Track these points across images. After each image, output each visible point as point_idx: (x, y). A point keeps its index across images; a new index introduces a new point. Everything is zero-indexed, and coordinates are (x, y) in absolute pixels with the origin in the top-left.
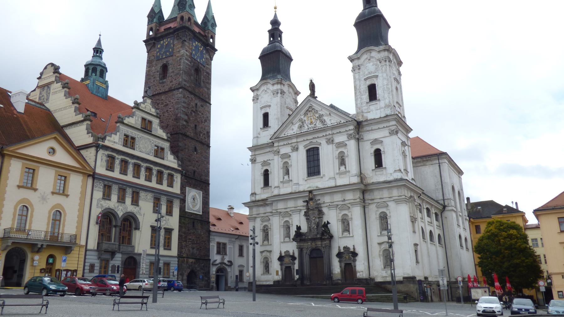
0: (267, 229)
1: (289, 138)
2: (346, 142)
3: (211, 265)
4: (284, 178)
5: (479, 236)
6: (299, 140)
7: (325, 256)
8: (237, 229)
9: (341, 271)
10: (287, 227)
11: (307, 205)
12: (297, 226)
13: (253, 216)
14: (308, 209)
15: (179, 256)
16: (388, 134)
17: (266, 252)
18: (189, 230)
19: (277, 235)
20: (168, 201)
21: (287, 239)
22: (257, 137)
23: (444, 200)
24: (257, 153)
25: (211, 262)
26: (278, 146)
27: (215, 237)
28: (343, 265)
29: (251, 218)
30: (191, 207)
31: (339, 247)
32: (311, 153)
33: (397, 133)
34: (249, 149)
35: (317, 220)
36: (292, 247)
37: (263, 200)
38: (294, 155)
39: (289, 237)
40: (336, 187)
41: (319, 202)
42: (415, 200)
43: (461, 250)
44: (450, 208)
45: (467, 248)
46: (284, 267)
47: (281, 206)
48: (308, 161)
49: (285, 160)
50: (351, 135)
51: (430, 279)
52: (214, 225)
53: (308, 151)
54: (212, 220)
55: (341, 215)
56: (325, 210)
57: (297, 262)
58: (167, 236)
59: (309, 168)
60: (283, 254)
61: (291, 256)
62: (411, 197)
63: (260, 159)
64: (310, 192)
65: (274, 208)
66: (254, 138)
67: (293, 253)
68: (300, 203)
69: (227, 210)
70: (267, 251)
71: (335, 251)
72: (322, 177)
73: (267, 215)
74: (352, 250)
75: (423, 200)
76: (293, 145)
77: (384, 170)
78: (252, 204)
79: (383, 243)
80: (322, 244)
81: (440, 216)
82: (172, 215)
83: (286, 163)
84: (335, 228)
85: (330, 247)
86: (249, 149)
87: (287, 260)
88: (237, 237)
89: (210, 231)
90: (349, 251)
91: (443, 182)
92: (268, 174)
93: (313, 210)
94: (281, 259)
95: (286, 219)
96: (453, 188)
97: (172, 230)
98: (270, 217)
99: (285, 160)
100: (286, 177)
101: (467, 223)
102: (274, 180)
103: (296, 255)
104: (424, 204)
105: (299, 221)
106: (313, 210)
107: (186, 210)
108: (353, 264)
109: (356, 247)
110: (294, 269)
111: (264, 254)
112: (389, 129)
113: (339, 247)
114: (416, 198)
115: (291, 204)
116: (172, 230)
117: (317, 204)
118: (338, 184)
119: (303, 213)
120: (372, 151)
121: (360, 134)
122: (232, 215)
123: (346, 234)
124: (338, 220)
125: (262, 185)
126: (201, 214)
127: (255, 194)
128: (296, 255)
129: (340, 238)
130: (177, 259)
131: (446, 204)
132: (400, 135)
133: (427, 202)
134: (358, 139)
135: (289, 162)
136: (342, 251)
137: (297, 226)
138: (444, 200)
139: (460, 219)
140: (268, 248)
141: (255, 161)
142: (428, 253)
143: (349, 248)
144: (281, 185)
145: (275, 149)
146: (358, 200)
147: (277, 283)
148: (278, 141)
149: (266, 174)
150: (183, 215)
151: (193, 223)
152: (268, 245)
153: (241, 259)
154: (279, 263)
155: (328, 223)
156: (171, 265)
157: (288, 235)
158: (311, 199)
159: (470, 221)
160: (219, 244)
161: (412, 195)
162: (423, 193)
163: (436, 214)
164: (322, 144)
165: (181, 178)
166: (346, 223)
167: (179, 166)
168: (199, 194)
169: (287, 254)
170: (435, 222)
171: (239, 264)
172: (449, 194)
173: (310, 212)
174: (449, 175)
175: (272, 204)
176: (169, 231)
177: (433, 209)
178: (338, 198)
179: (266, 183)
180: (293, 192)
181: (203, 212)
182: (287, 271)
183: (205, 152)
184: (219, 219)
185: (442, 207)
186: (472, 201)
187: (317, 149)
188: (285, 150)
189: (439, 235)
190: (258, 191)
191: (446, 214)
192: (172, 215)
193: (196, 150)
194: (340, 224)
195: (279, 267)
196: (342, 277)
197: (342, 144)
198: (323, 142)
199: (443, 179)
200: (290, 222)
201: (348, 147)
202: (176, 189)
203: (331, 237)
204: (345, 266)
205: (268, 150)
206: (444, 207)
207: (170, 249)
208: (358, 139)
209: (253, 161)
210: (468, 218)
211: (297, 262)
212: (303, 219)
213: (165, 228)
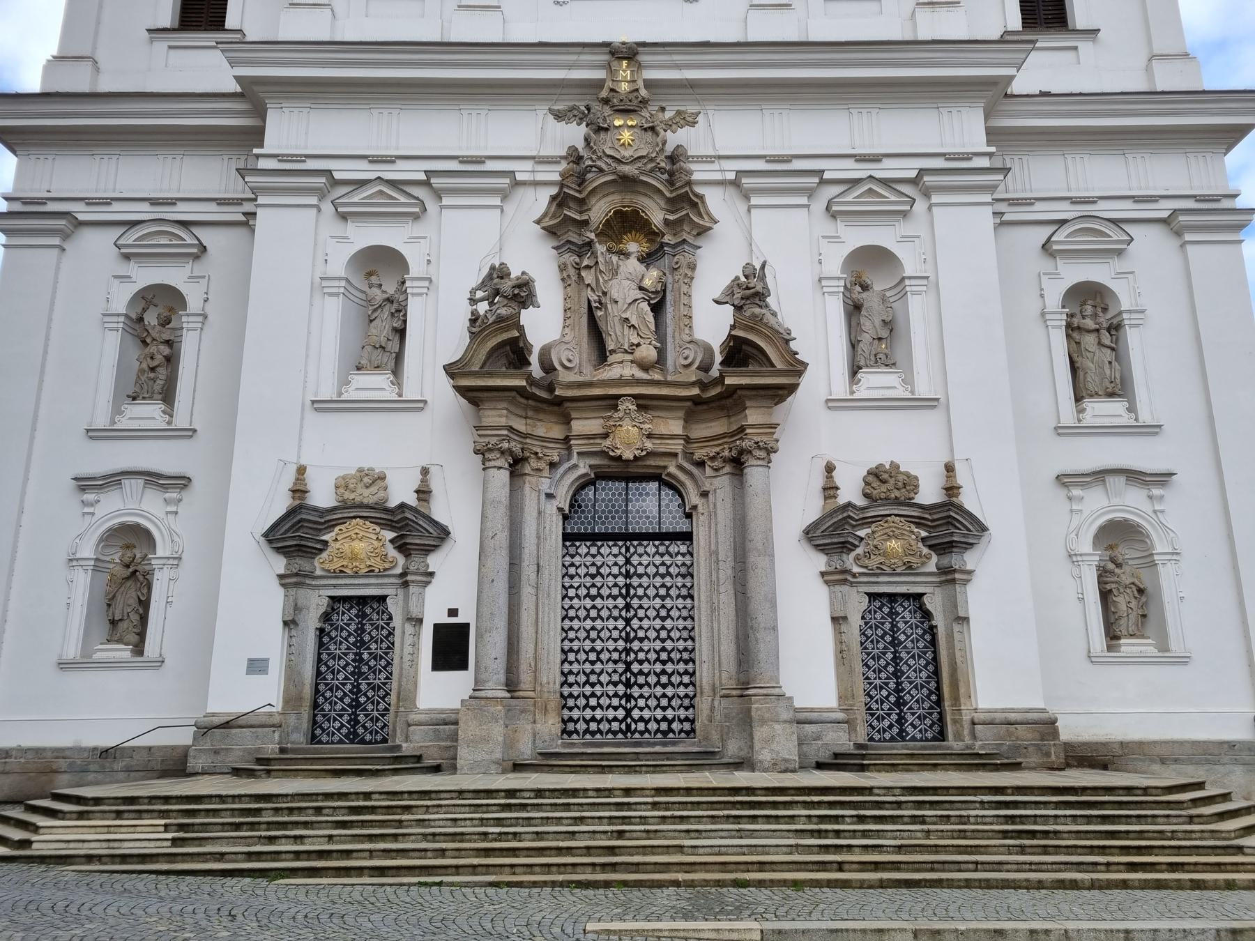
10: (380, 300)
11: (587, 140)
17: (132, 486)
28: (856, 604)
46: (316, 602)
56: (715, 200)
60: (322, 496)
70: (153, 478)
74: (929, 493)
77: (1085, 47)
79: (1100, 476)
93: (626, 183)
98: (207, 236)
109: (962, 478)
110: (420, 621)
137: (499, 273)
143: (911, 484)
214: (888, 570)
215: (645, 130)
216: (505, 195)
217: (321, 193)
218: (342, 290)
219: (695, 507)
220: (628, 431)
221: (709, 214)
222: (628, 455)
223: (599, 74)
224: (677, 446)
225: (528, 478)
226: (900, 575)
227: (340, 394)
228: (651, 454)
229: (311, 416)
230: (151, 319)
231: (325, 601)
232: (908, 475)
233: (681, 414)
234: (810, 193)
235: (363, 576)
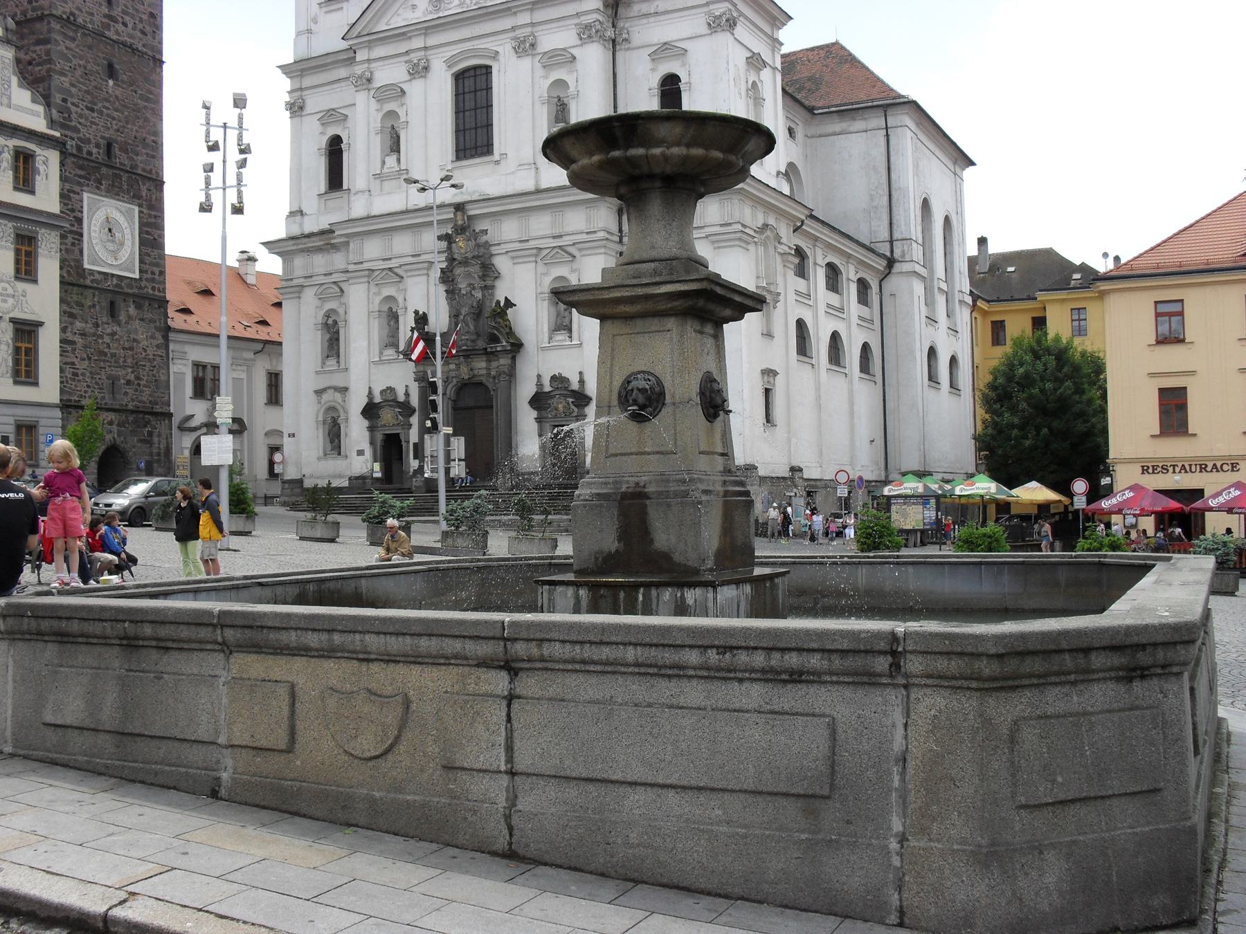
0: (335, 322)
1: (401, 34)
2: (573, 51)
3: (175, 430)
4: (384, 163)
5: (1000, 352)
6: (432, 40)
7: (498, 403)
8: (264, 323)
9: (543, 447)
11: (449, 248)
12: (416, 312)
13: (295, 282)
14: (451, 259)
15: (68, 406)
16: (704, 29)
17: (331, 392)
18: (97, 325)
19: (361, 338)
20: (18, 236)
21: (390, 352)
22: (309, 31)
23: (891, 242)
24: (307, 82)
25: (176, 421)
26: (369, 61)
27: (187, 348)
29: (289, 287)
30: (103, 254)
31: (539, 376)
32: (469, 84)
33: (731, 24)
34: (285, 69)
35: (479, 295)
36: (400, 378)
37: (322, 233)
38: (415, 89)
39: (395, 345)
40: (538, 191)
41: (484, 238)
42: (778, 239)
43: (931, 394)
44: (906, 267)
45: (953, 385)
46: (379, 437)
47: (372, 250)
48: (459, 111)
49: (389, 106)
50: (588, 27)
51: (811, 473)
52: (186, 311)
53: (459, 77)
54: (176, 294)
56: (501, 263)
57: (415, 420)
58: (23, 345)
59: (460, 131)
60: (378, 399)
61: (400, 405)
62: (766, 226)
63: (317, 102)
64: (459, 207)
65: (352, 258)
66: (299, 34)
67: (407, 394)
68: (429, 241)
69: (236, 265)
70: (336, 389)
71: (526, 390)
72: (497, 162)
73: (335, 277)
75: (816, 239)
76: (414, 57)
78: (290, 246)
80: (488, 369)
81: (874, 285)
82: (35, 281)
83: (392, 114)
85: (511, 374)
86: (285, 69)
88: (259, 347)
89: (169, 329)
90: (566, 389)
91: (894, 186)
92: (341, 151)
93: (465, 263)
94: (370, 411)
95: (388, 291)
96: (926, 204)
97: (41, 324)
98: (344, 286)
99: (389, 106)
100: (391, 161)
101: (964, 316)
102: (357, 169)
103: (415, 401)
104: (819, 252)
105: (425, 296)
106: (465, 263)
107: (86, 266)
110: (408, 442)
111: (325, 397)
112: (709, 14)
113: (539, 376)
114: (784, 231)
115: (402, 244)
116: (41, 324)
117: (478, 246)
118: (544, 185)
119: (436, 274)
120: (655, 81)
121: (621, 24)
122: (251, 280)
123: (561, 337)
125: (323, 186)
126: (137, 276)
127: (301, 213)
128: (415, 401)
129: (543, 349)
130: (58, 413)
131: (897, 253)
132: (741, 31)
133: (830, 247)
134: (614, 41)
135: (401, 112)
136: (547, 388)
137: (416, 312)
138: (891, 242)
139: (941, 301)
140: (338, 380)
141: (301, 108)
142: (818, 398)
144: (375, 186)
145: (358, 70)
146: (601, 234)
147: (360, 483)
148: (370, 45)
149: (335, 151)
150: (75, 280)
151: (112, 304)
152: (339, 371)
153: (273, 410)
154: (366, 423)
155: (509, 304)
156: (41, 430)
157: (391, 340)
158: (461, 230)
159: (974, 307)
160: (197, 365)
161: (771, 221)
162: (812, 217)
163: (863, 285)
164: (501, 57)
165: (62, 164)
167: (52, 123)
168: (128, 215)
170: (854, 308)
171: (268, 429)
172: (908, 225)
173: (459, 271)
174: (916, 166)
175: (348, 243)
176: (26, 331)
177: (852, 269)
178: (541, 225)
179: (335, 179)
180: (411, 207)
181: (141, 271)
182: (391, 449)
183: (146, 79)
184: (207, 293)
185: (884, 263)
186: (994, 248)
187: (488, 69)
188: (388, 74)
189: (866, 348)
190: (311, 205)
191: (893, 283)
192: (35, 281)
193: (111, 72)
194: (546, 303)
195: (366, 435)
197: (563, 58)
198: (505, 47)
199: (893, 176)
200: (400, 300)
201: (579, 65)
202: (46, 196)
203: (517, 346)
205: (342, 72)
206: (891, 262)
207: (36, 384)
208: (614, 41)
209: (296, 108)
210: (969, 300)
211: (415, 420)
213: (13, 320)
216: (428, 269)
217: (369, 276)
223: (452, 216)
224: (484, 372)
230: (330, 322)
234: (536, 256)
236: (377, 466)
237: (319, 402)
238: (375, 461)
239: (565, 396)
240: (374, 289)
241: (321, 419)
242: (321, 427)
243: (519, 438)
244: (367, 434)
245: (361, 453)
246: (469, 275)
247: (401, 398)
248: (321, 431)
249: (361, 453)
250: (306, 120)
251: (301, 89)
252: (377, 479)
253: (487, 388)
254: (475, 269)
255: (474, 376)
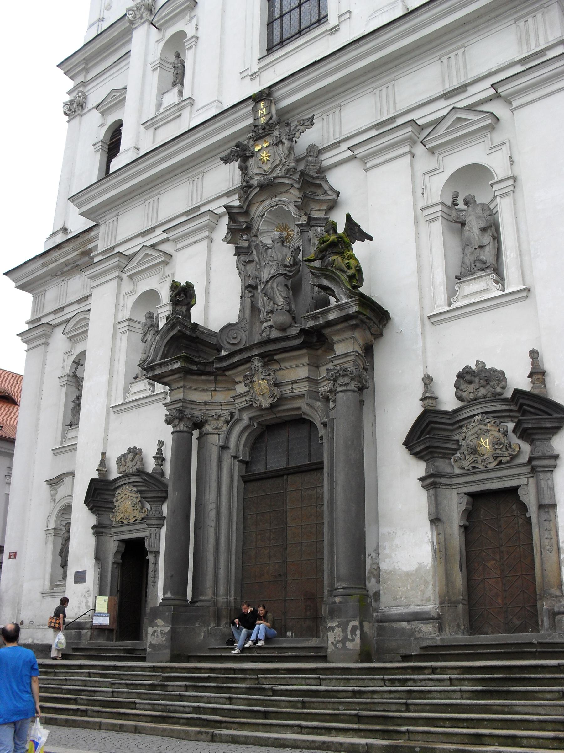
9: (441, 553)
28: (455, 505)
31: (428, 381)
46: (112, 546)
55: (438, 183)
67: (160, 458)
84: (399, 247)
87: (126, 502)
90: (497, 397)
93: (269, 187)
106: (269, 187)
108: (529, 497)
109: (548, 365)
113: (428, 381)
124: (423, 214)
129: (435, 319)
136: (448, 401)
141: (81, 106)
154: (92, 520)
155: (355, 231)
166: (474, 225)
169: (132, 467)
194: (438, 226)
196: (446, 601)
204: (469, 515)
212: (225, 256)
214: (481, 467)
215: (276, 145)
218: (127, 328)
219: (322, 438)
220: (259, 384)
221: (332, 189)
222: (266, 403)
224: (303, 388)
225: (209, 436)
226: (493, 470)
227: (125, 399)
228: (282, 399)
229: (113, 416)
231: (117, 544)
232: (493, 370)
233: (306, 360)
235: (132, 524)
236: (103, 604)
237: (53, 500)
238: (101, 593)
239: (498, 416)
240: (127, 286)
241: (52, 526)
242: (51, 539)
243: (383, 530)
244: (92, 540)
245: (80, 577)
246: (279, 212)
247: (151, 465)
248: (50, 546)
249: (80, 577)
250: (86, 118)
251: (84, 84)
252: (101, 629)
253: (311, 424)
254: (289, 199)
255: (282, 399)
